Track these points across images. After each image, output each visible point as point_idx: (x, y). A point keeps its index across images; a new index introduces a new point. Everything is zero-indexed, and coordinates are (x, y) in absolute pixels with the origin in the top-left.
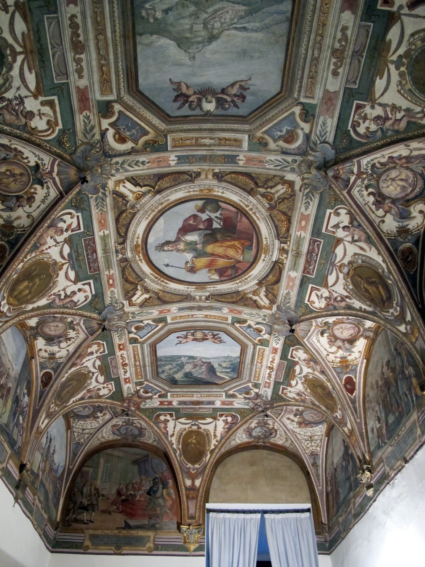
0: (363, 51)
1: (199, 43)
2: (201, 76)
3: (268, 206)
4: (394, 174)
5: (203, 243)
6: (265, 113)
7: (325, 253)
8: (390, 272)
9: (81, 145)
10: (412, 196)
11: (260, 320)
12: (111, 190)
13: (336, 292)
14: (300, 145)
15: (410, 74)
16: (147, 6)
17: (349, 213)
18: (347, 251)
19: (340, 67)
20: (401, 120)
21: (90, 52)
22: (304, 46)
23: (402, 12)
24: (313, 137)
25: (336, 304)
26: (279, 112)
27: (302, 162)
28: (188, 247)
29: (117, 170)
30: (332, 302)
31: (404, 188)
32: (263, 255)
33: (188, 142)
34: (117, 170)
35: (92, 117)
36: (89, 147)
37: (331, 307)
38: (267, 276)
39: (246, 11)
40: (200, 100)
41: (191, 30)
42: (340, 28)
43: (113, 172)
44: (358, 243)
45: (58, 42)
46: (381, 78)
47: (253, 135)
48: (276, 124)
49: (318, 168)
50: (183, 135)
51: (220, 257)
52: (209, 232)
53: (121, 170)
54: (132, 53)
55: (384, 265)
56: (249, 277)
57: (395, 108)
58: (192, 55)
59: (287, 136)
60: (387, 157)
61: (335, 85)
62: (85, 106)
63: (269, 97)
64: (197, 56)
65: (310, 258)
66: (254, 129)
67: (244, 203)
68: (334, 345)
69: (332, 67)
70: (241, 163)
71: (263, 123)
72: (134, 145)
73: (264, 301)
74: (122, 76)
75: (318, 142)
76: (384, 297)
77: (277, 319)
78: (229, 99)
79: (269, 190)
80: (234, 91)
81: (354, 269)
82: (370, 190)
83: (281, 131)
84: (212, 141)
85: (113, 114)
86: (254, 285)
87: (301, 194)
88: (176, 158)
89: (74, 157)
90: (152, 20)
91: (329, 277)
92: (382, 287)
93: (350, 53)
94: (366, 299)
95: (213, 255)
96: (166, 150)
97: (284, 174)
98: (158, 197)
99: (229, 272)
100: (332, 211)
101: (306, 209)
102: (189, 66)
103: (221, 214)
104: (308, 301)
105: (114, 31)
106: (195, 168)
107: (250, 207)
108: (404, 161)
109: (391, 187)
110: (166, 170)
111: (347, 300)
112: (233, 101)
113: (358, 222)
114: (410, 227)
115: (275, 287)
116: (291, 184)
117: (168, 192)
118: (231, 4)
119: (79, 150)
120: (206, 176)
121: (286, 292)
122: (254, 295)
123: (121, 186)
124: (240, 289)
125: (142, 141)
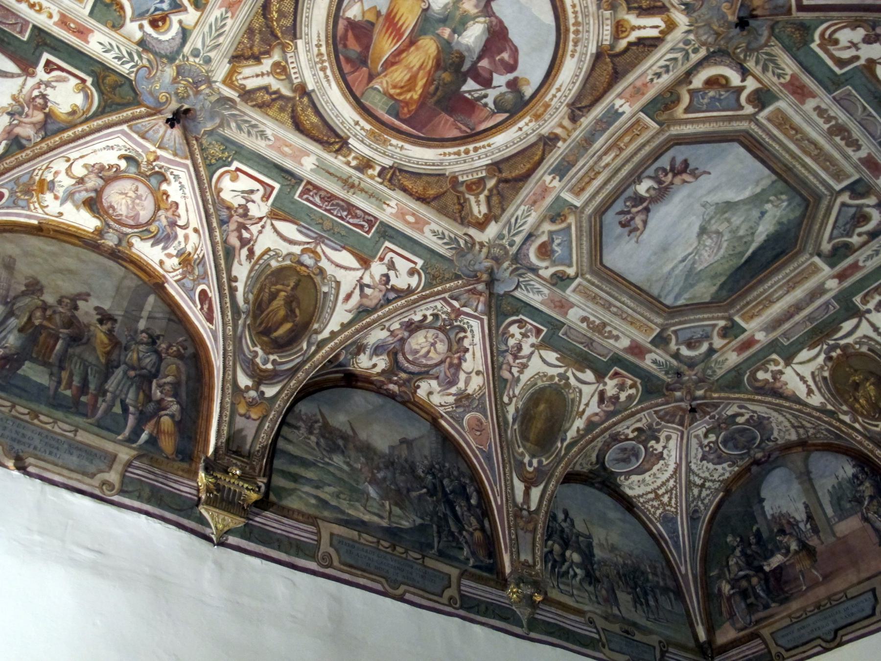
0: (589, 349)
1: (711, 218)
2: (681, 201)
3: (461, 179)
4: (442, 347)
5: (448, 43)
6: (591, 239)
7: (343, 233)
8: (321, 344)
9: (768, 40)
10: (400, 358)
11: (195, 41)
12: (672, 10)
13: (260, 232)
14: (529, 258)
15: (550, 386)
16: (785, 204)
17: (409, 291)
18: (341, 267)
19: (588, 326)
20: (510, 372)
21: (820, 134)
22: (629, 302)
23: (601, 385)
24: (530, 275)
25: (233, 226)
26: (582, 253)
27: (507, 253)
28: (458, 14)
29: (687, 42)
30: (236, 218)
31: (416, 352)
32: (368, 127)
33: (627, 139)
34: (687, 42)
35: (775, 79)
36: (754, 45)
37: (224, 213)
38: (317, 113)
39: (695, 268)
40: (660, 182)
41: (728, 220)
42: (620, 335)
43: (691, 37)
44: (357, 291)
45: (864, 122)
46: (557, 359)
47: (575, 213)
48: (571, 242)
49: (491, 272)
50: (640, 140)
51: (399, 53)
52: (466, 67)
53: (681, 45)
54: (771, 164)
55: (325, 334)
56: (326, 77)
57: (524, 366)
58: (708, 206)
59: (549, 248)
60: (471, 348)
61: (574, 316)
62: (793, 85)
63: (605, 252)
64: (704, 209)
65: (338, 205)
66: (581, 217)
67: (484, 147)
68: (90, 172)
69: (592, 318)
70: (548, 178)
71: (581, 231)
72: (691, 87)
73: (253, 76)
74: (767, 140)
75: (521, 279)
76: (276, 334)
77: (196, 84)
78: (634, 210)
79: (486, 192)
80: (638, 221)
81: (309, 276)
82: (430, 318)
83: (559, 245)
84: (603, 164)
85: (749, 100)
86: (302, 76)
87: (460, 233)
88: (620, 110)
89: (769, 23)
90: (772, 198)
91: (294, 227)
92: (291, 330)
93: (595, 338)
94: (255, 291)
95: (412, 42)
96: (643, 110)
97: (500, 224)
98: (592, 49)
99: (354, 47)
100: (418, 267)
101: (434, 230)
102: (701, 197)
103: (486, 105)
104: (238, 169)
105: (805, 165)
106: (587, 121)
107: (472, 153)
108: (456, 361)
109: (424, 340)
110: (619, 88)
111: (245, 252)
112: (629, 212)
113: (394, 299)
114: (362, 354)
115: (286, 117)
116: (481, 225)
117: (586, 66)
118: (713, 261)
119: (766, 33)
120: (563, 127)
121: (269, 132)
122: (276, 65)
123: (663, 26)
124: (300, 43)
125: (686, 99)
